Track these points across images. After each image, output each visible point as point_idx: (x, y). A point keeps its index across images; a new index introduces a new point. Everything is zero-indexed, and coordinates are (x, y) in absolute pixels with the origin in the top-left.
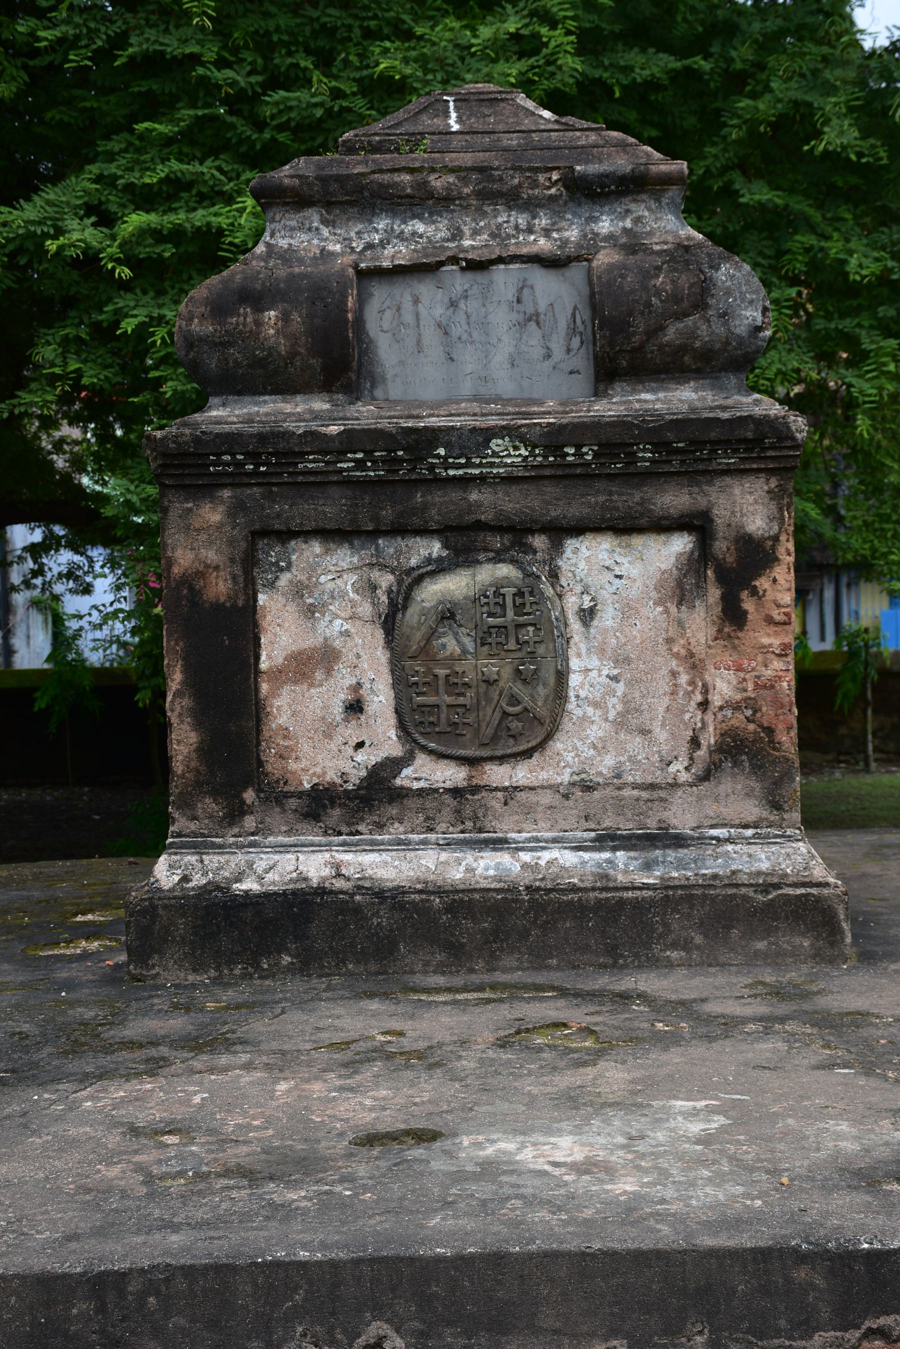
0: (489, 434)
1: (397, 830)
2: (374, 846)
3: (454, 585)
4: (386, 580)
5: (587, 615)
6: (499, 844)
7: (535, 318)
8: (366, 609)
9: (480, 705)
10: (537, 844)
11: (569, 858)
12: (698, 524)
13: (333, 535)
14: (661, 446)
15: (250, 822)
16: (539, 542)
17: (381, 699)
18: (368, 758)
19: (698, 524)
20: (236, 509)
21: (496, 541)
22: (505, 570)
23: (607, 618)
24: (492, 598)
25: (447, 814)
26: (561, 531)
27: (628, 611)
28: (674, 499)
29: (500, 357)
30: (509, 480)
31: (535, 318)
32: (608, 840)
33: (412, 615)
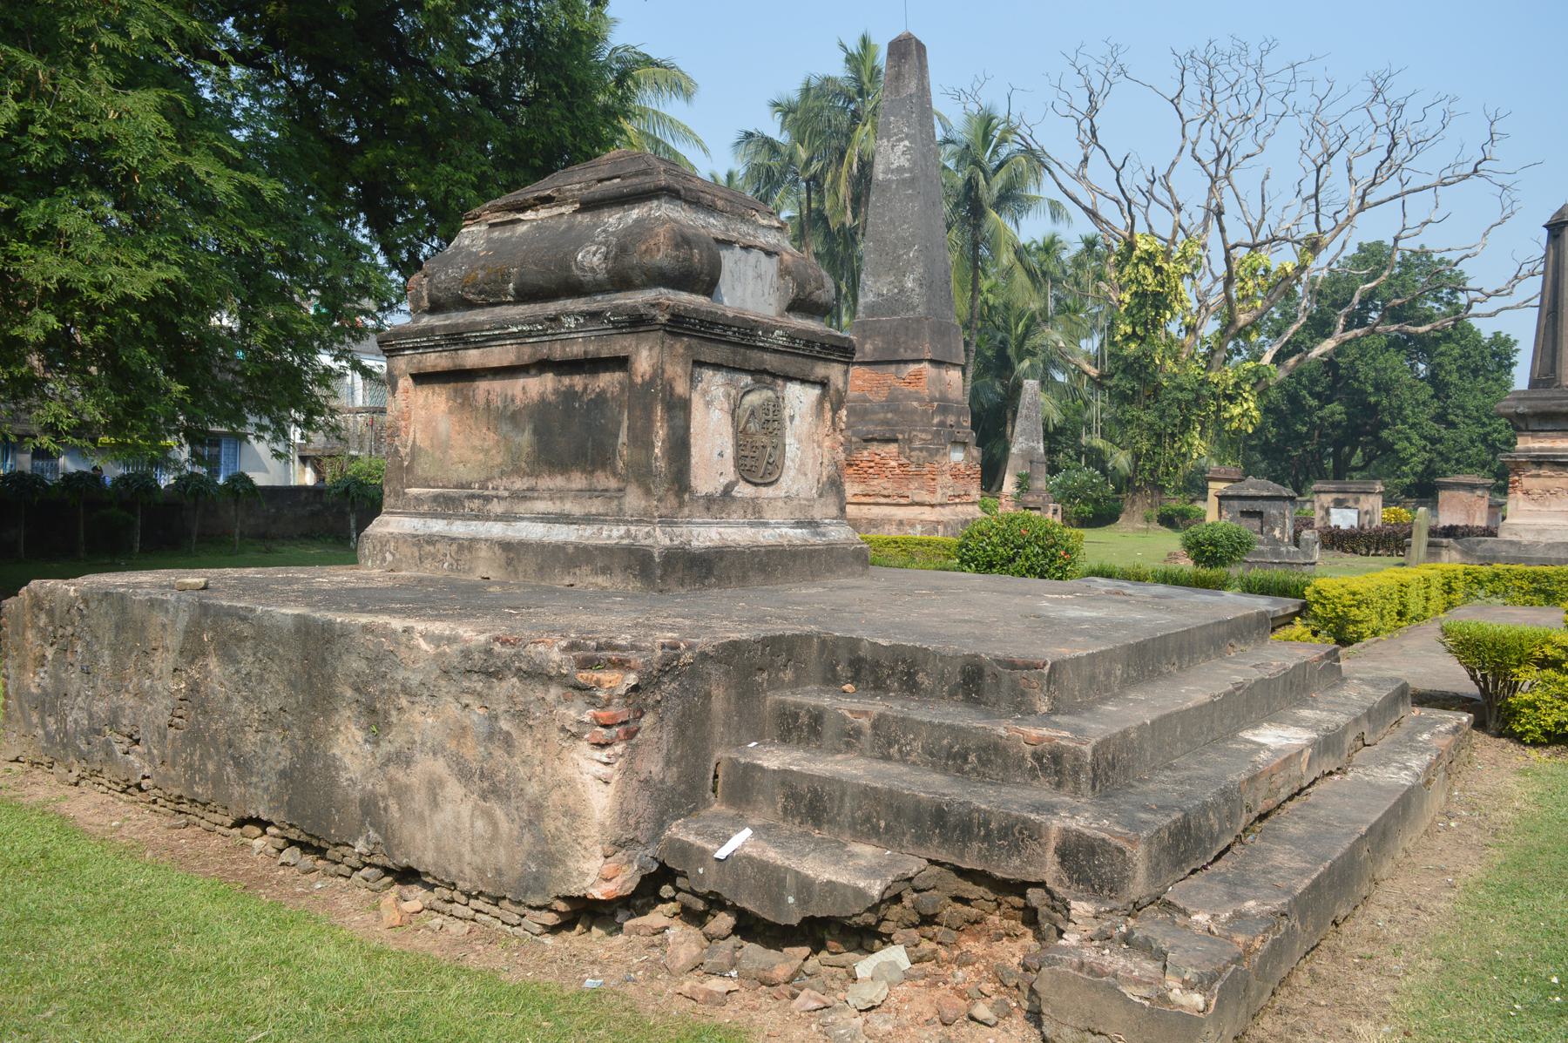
0: (776, 328)
1: (734, 518)
2: (730, 525)
3: (754, 399)
4: (733, 392)
5: (792, 418)
6: (766, 525)
7: (760, 276)
8: (726, 406)
9: (757, 459)
10: (778, 525)
11: (791, 532)
12: (823, 384)
13: (717, 367)
14: (823, 346)
15: (686, 511)
16: (780, 382)
17: (729, 452)
18: (724, 481)
19: (823, 384)
20: (689, 347)
21: (768, 379)
22: (770, 394)
23: (797, 421)
24: (764, 407)
25: (750, 511)
26: (789, 378)
27: (802, 417)
28: (820, 370)
29: (749, 292)
30: (776, 351)
31: (760, 276)
32: (799, 524)
33: (739, 412)
